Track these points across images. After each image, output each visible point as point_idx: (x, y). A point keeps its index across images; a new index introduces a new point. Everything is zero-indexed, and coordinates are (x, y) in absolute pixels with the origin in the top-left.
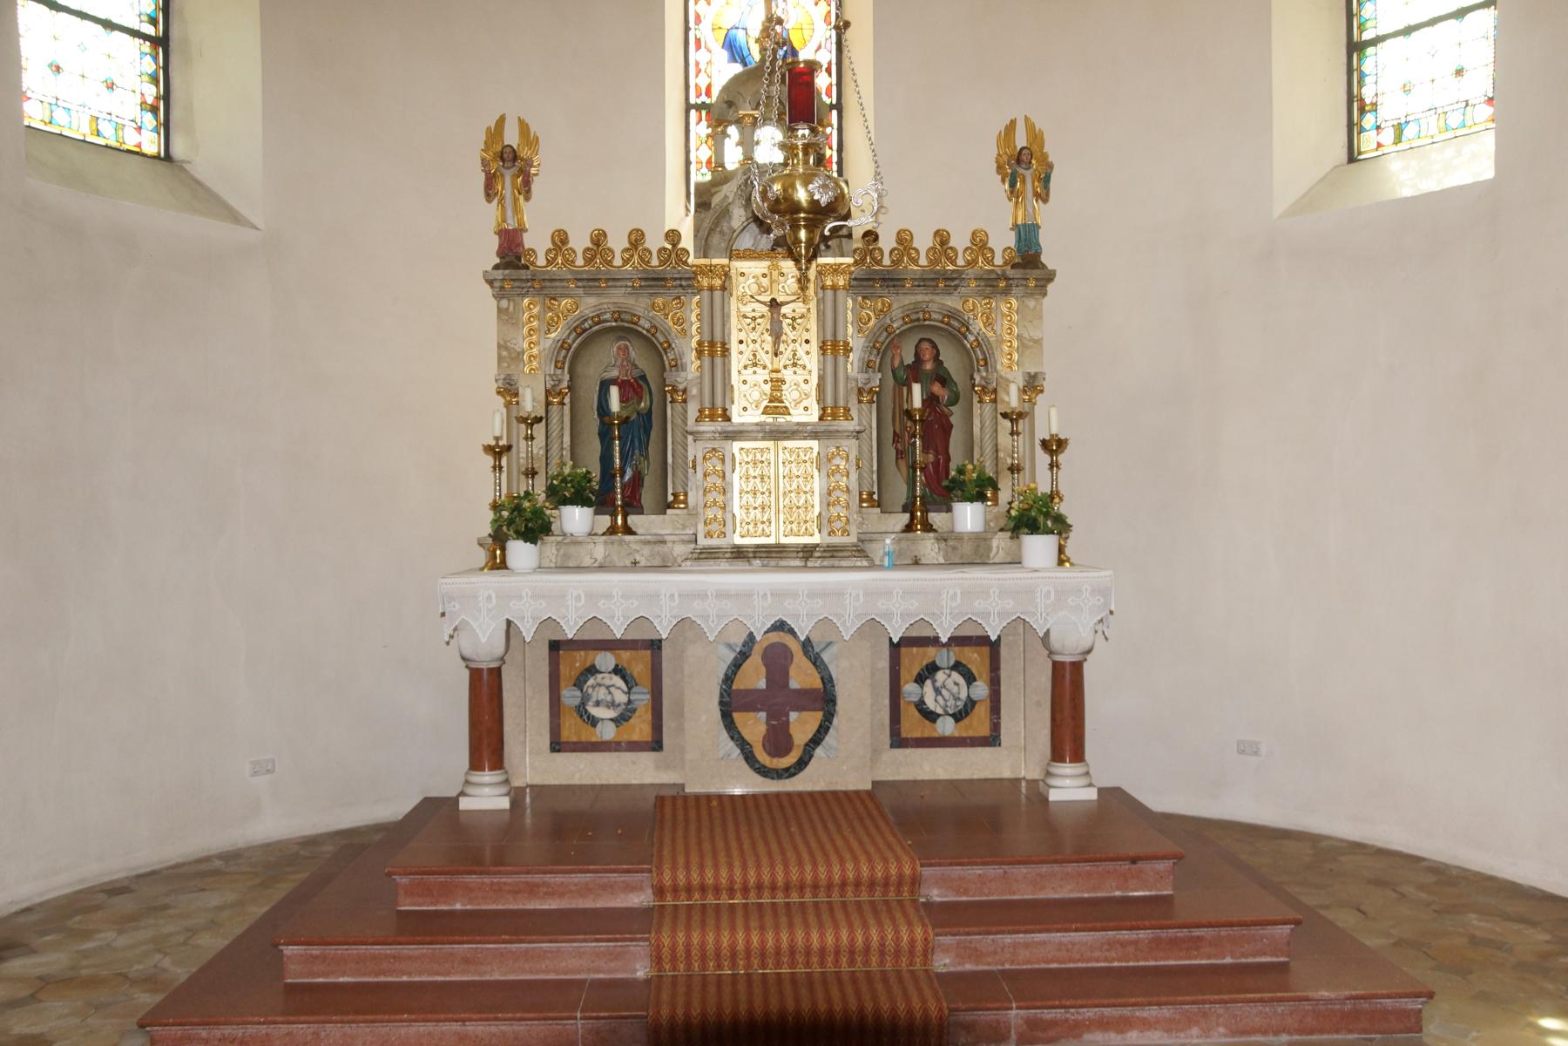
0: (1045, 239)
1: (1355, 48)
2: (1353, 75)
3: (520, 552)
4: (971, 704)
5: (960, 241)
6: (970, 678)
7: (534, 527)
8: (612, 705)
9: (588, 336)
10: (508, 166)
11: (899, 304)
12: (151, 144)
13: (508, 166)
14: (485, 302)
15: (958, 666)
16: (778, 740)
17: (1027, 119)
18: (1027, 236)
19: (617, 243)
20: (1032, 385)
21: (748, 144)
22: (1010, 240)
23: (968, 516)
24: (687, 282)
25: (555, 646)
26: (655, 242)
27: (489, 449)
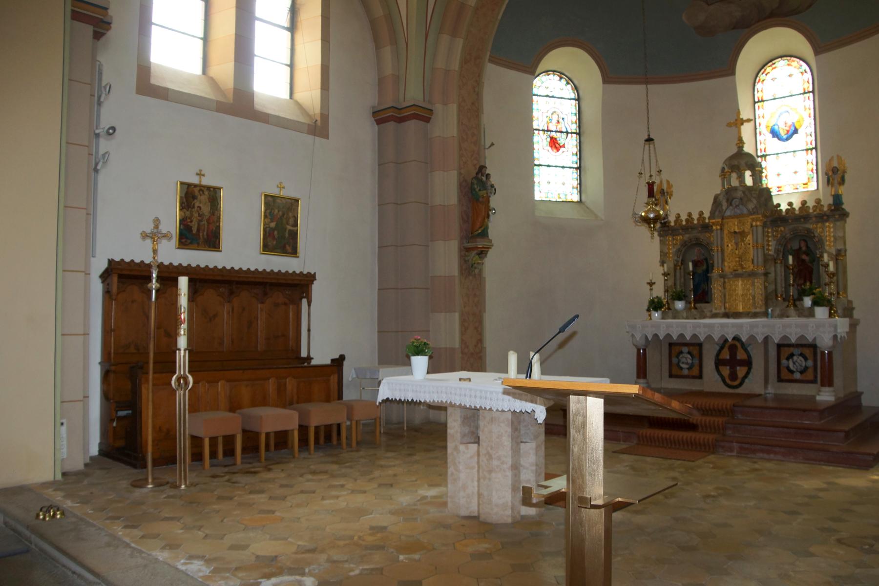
0: (844, 200)
3: (656, 315)
4: (806, 368)
6: (806, 359)
8: (687, 363)
9: (687, 247)
12: (576, 198)
15: (801, 355)
16: (733, 376)
17: (838, 156)
18: (837, 200)
22: (830, 201)
25: (670, 345)
27: (648, 283)
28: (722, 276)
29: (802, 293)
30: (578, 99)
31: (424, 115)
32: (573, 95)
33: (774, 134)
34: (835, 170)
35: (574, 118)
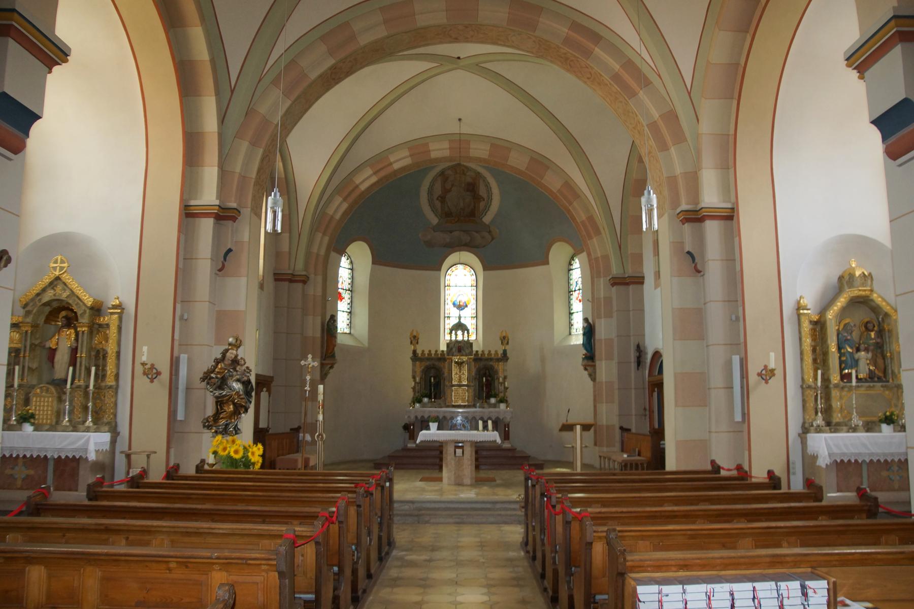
1: (571, 314)
2: (570, 319)
5: (493, 352)
7: (420, 401)
10: (415, 339)
11: (482, 364)
12: (347, 331)
13: (415, 339)
14: (410, 362)
18: (505, 352)
19: (433, 352)
20: (505, 378)
21: (456, 335)
23: (493, 400)
24: (445, 360)
26: (439, 353)
29: (489, 396)
30: (352, 269)
31: (304, 281)
32: (350, 267)
33: (454, 304)
34: (504, 338)
35: (350, 281)
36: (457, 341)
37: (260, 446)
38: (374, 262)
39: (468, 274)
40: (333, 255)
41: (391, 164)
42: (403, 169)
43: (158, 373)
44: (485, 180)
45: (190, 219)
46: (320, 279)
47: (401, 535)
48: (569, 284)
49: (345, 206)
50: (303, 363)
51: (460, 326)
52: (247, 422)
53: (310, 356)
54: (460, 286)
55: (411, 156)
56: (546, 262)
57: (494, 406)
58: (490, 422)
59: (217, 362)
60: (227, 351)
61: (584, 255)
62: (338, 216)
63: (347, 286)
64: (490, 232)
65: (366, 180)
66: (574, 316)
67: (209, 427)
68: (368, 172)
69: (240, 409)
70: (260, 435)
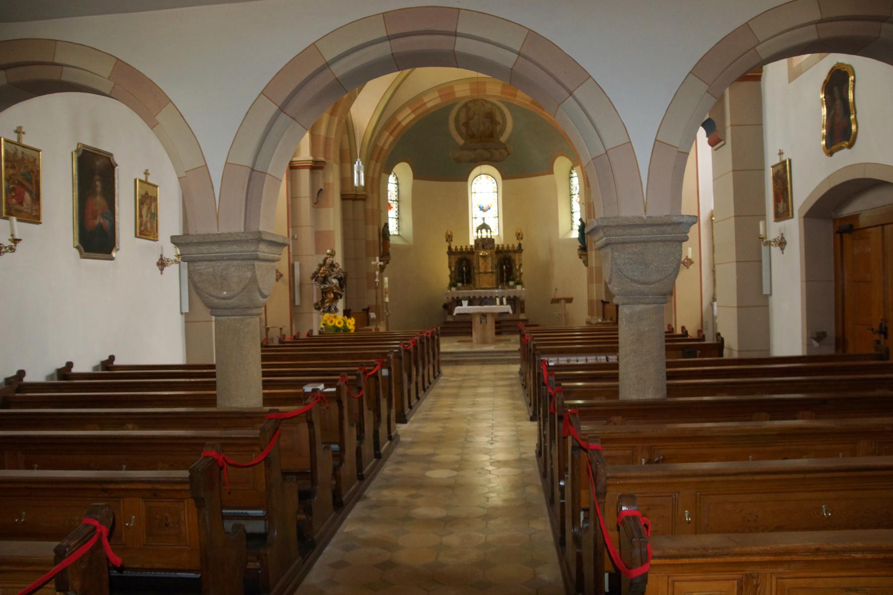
1: (572, 213)
2: (572, 217)
3: (453, 289)
7: (455, 286)
10: (449, 238)
11: (501, 256)
12: (396, 233)
14: (447, 256)
18: (520, 245)
19: (464, 247)
20: (520, 265)
23: (511, 283)
28: (480, 273)
29: (508, 281)
30: (397, 184)
31: (364, 199)
33: (482, 209)
36: (482, 239)
37: (353, 319)
38: (414, 178)
39: (490, 182)
40: (384, 175)
41: (425, 104)
42: (435, 106)
43: (281, 275)
44: (499, 108)
45: (294, 171)
46: (375, 195)
47: (446, 370)
48: (570, 189)
49: (391, 138)
50: (373, 263)
51: (484, 226)
52: (340, 305)
53: (378, 258)
54: (484, 192)
55: (440, 96)
56: (551, 172)
57: (513, 287)
58: (504, 299)
59: (321, 266)
60: (327, 258)
61: (579, 167)
62: (386, 147)
63: (394, 198)
64: (506, 149)
65: (406, 118)
66: (574, 215)
67: (318, 309)
68: (408, 111)
69: (336, 297)
70: (347, 313)
